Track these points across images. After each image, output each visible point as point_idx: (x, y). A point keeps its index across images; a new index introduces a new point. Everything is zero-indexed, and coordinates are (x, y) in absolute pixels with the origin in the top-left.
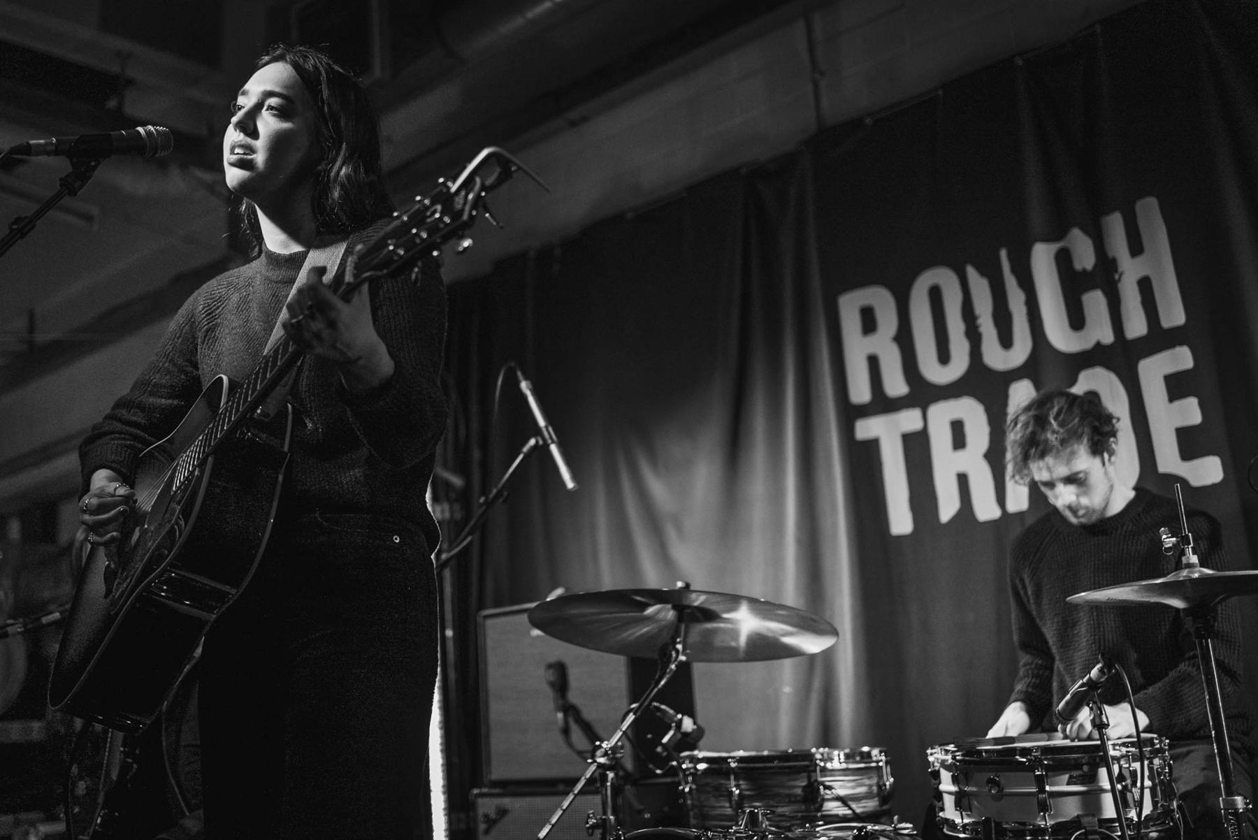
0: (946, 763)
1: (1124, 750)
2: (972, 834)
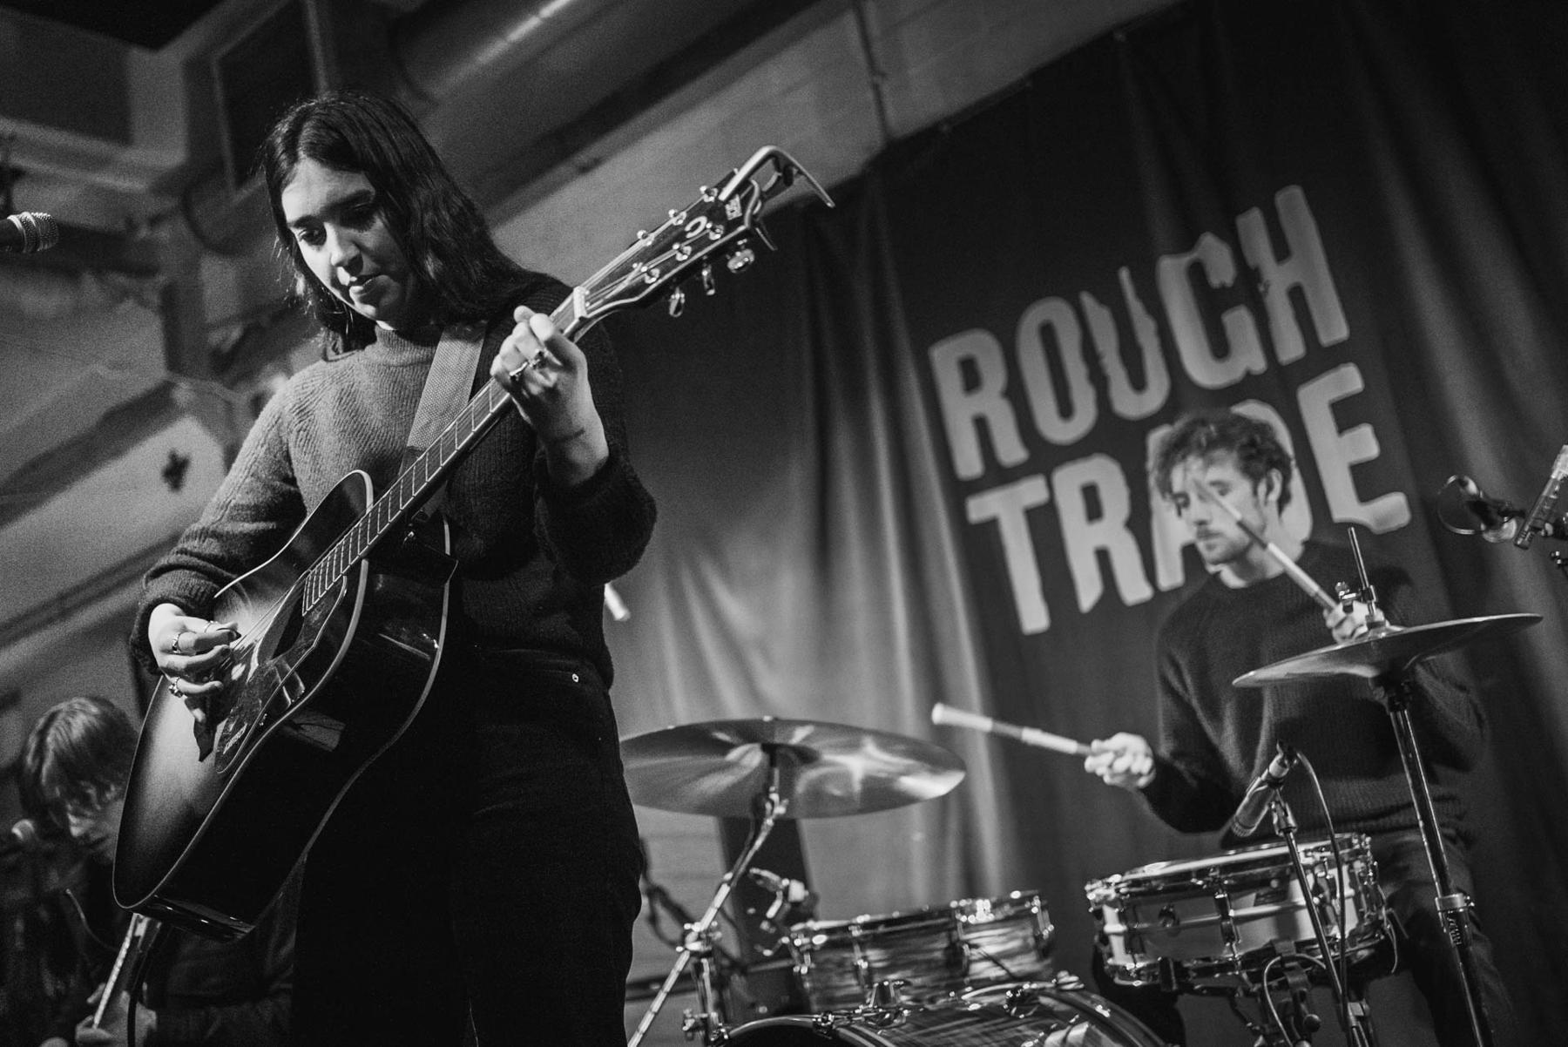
1: (1318, 855)
2: (1148, 980)
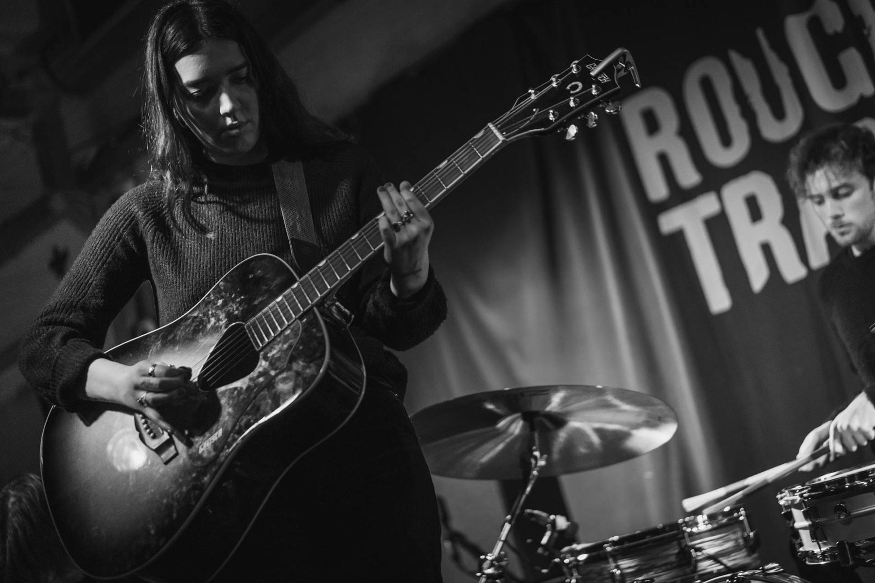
0: (795, 503)
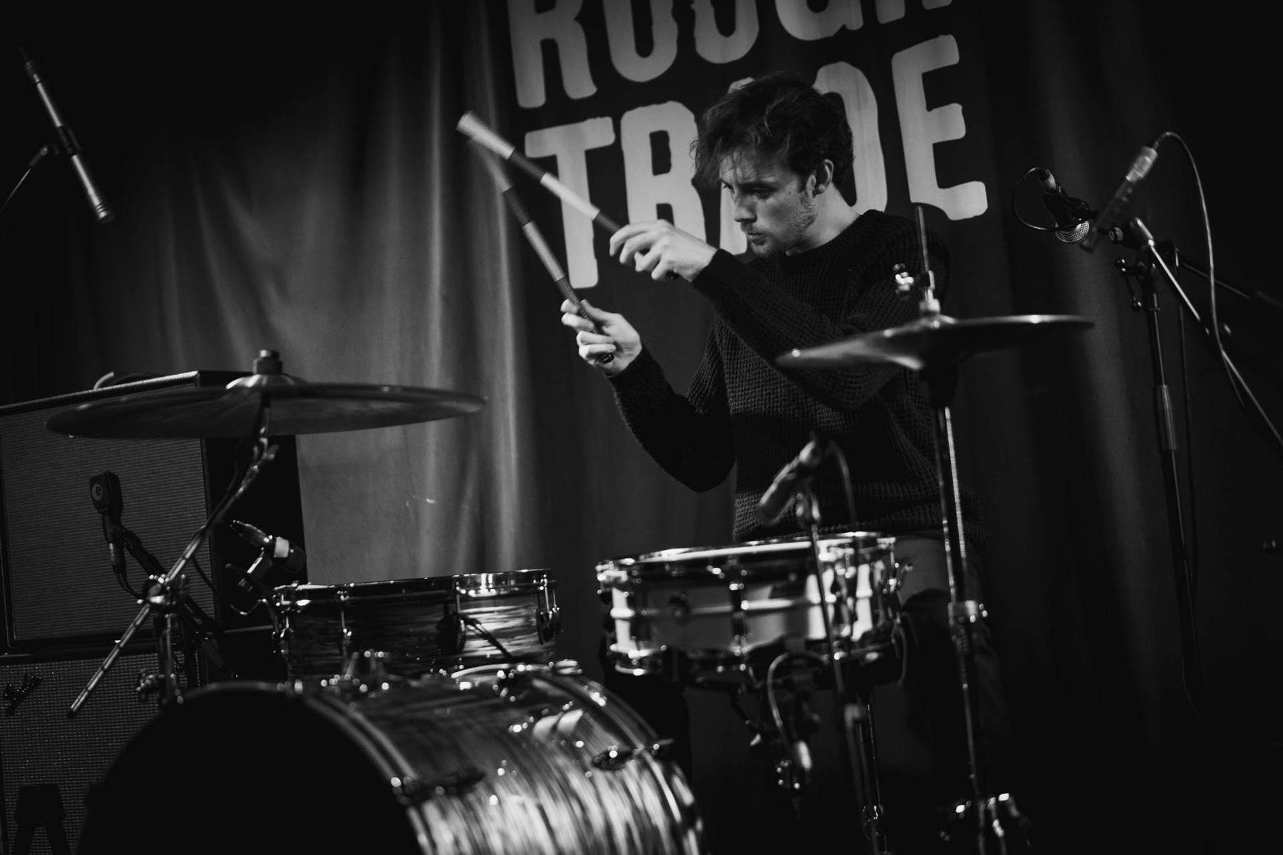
1: (840, 552)
